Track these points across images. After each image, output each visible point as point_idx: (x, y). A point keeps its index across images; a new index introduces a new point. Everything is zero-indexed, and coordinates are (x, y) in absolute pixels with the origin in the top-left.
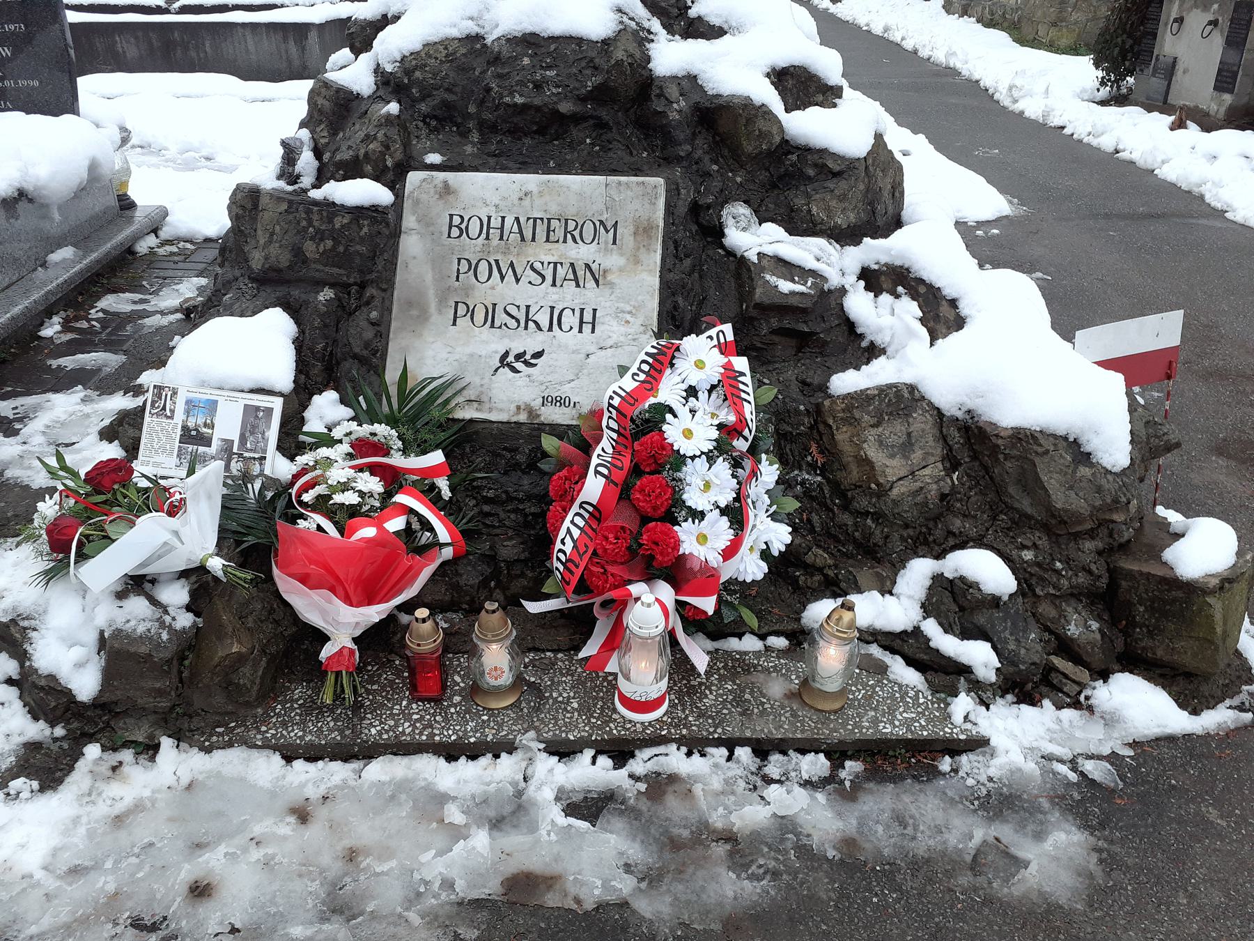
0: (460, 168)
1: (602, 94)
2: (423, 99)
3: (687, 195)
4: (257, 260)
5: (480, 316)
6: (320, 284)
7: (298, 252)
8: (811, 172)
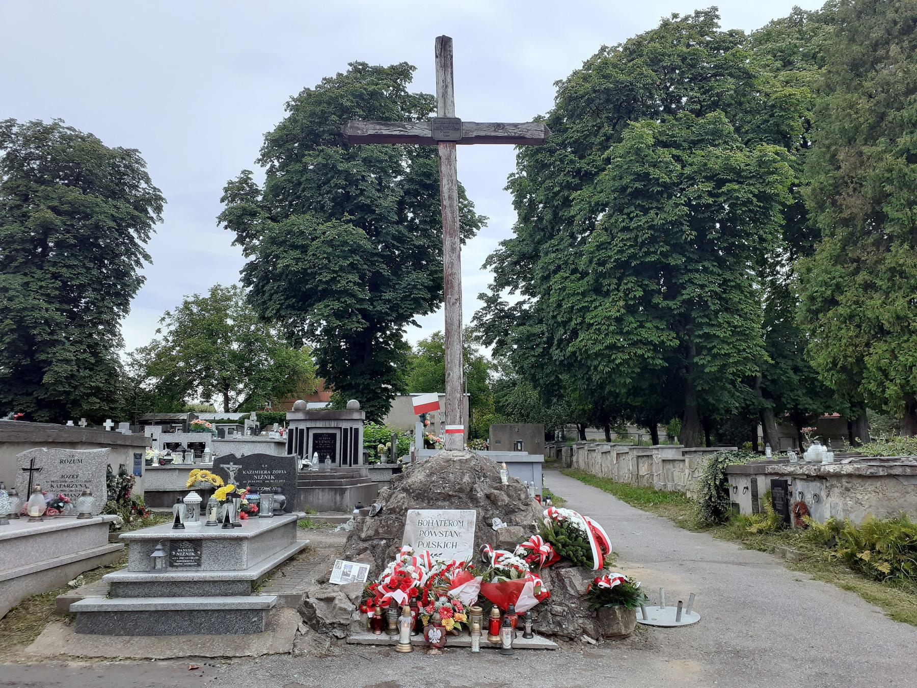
0: (422, 509)
1: (461, 490)
2: (413, 492)
3: (482, 513)
4: (363, 535)
5: (425, 545)
6: (382, 539)
7: (377, 531)
8: (516, 510)
